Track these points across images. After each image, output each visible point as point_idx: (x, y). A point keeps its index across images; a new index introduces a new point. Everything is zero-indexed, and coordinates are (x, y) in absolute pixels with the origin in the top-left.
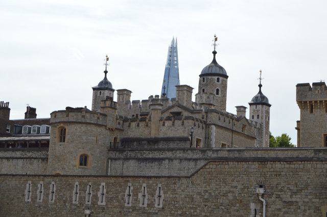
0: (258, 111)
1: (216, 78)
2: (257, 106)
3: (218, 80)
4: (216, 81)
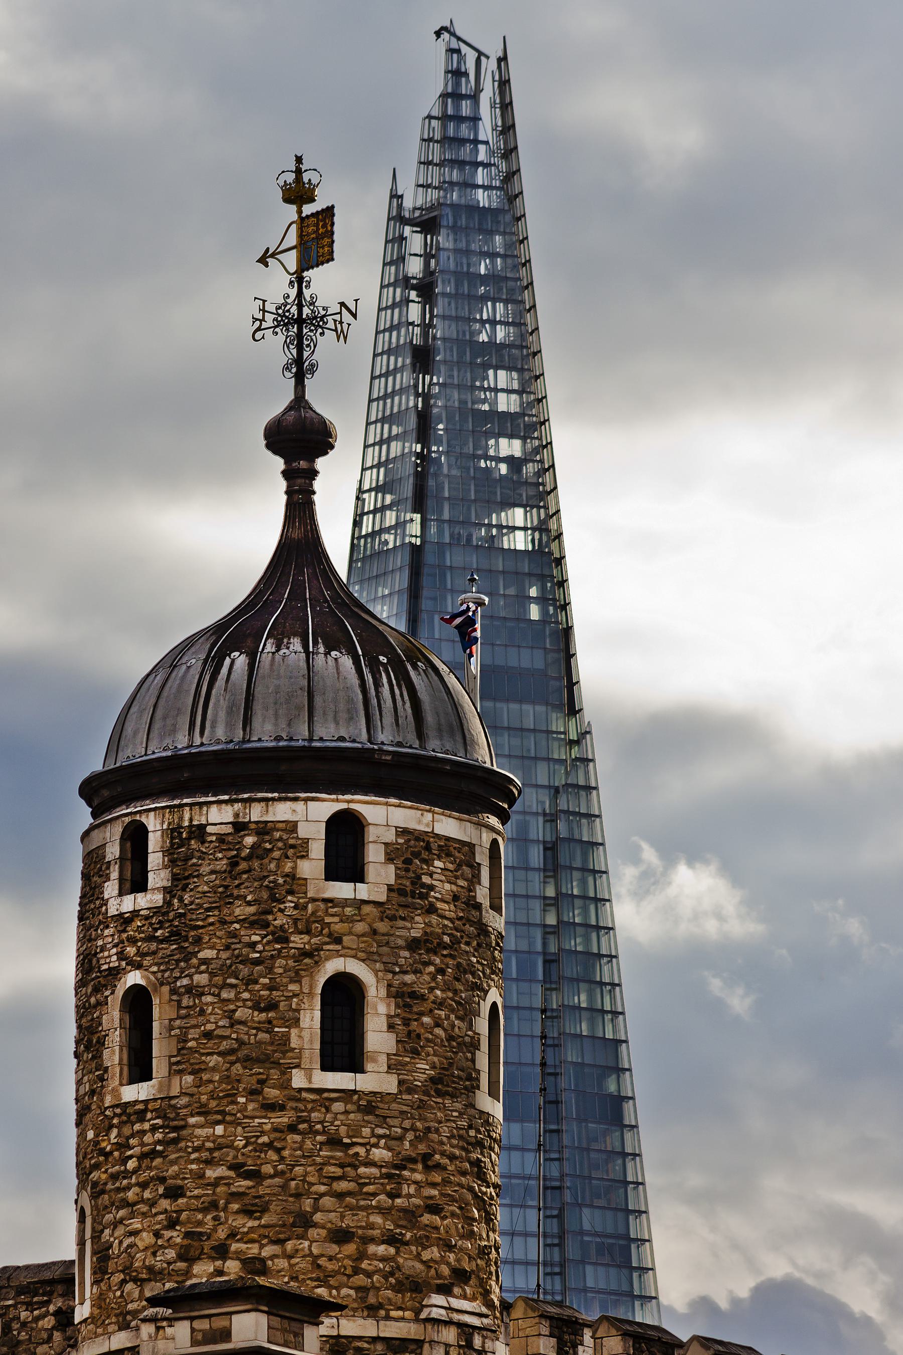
1: (312, 814)
4: (312, 867)
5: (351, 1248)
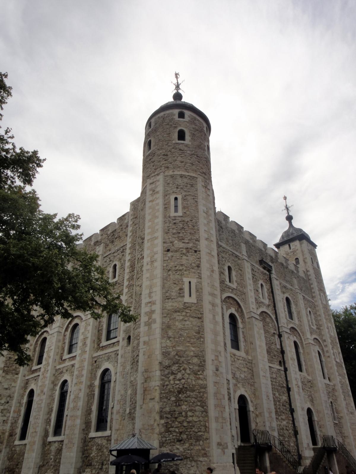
0: (294, 252)
2: (291, 244)
3: (181, 115)
5: (183, 163)
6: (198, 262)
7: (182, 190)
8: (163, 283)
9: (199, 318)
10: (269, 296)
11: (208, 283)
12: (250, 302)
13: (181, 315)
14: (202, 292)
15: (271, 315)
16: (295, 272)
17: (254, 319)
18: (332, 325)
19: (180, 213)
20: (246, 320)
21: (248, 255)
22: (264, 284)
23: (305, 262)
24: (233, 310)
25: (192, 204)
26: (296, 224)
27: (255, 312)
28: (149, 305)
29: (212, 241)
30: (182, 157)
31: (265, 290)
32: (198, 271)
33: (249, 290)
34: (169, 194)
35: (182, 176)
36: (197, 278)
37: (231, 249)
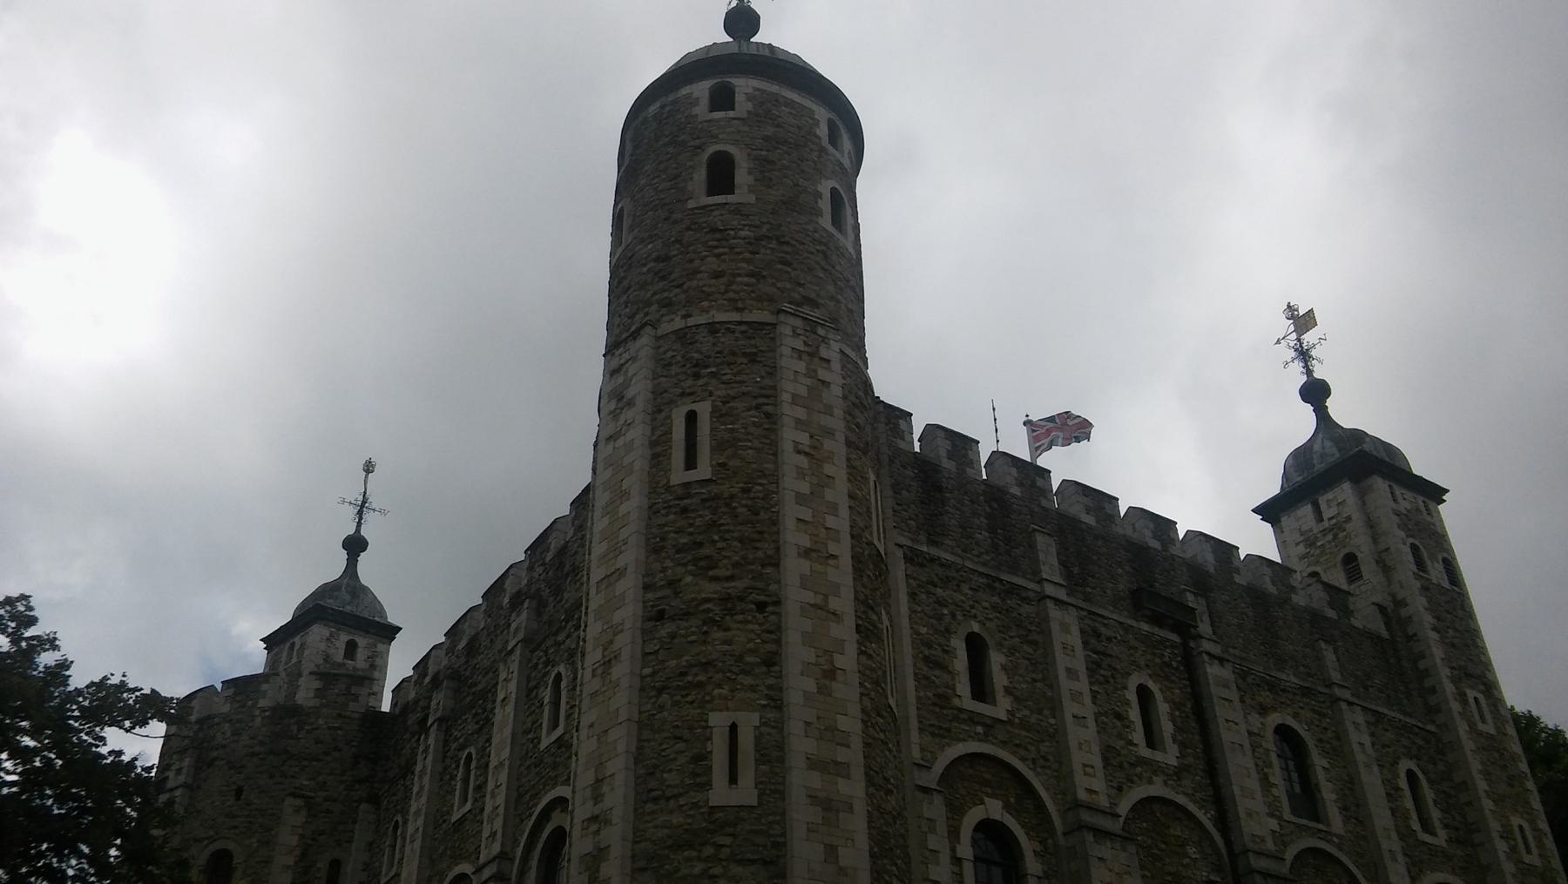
0: (1337, 528)
2: (1322, 501)
3: (722, 99)
5: (722, 280)
6: (772, 647)
7: (714, 381)
8: (639, 740)
9: (765, 863)
10: (1178, 729)
11: (807, 724)
12: (1077, 768)
13: (699, 859)
14: (782, 760)
15: (1192, 807)
16: (1331, 614)
17: (1090, 838)
18: (1532, 822)
19: (704, 470)
20: (1062, 840)
21: (1069, 575)
22: (1151, 684)
23: (1385, 568)
24: (994, 809)
25: (752, 429)
26: (1343, 412)
27: (1103, 802)
28: (594, 827)
29: (833, 556)
30: (718, 256)
31: (1163, 708)
32: (771, 681)
33: (1069, 718)
34: (671, 402)
35: (713, 328)
36: (764, 706)
37: (984, 564)
